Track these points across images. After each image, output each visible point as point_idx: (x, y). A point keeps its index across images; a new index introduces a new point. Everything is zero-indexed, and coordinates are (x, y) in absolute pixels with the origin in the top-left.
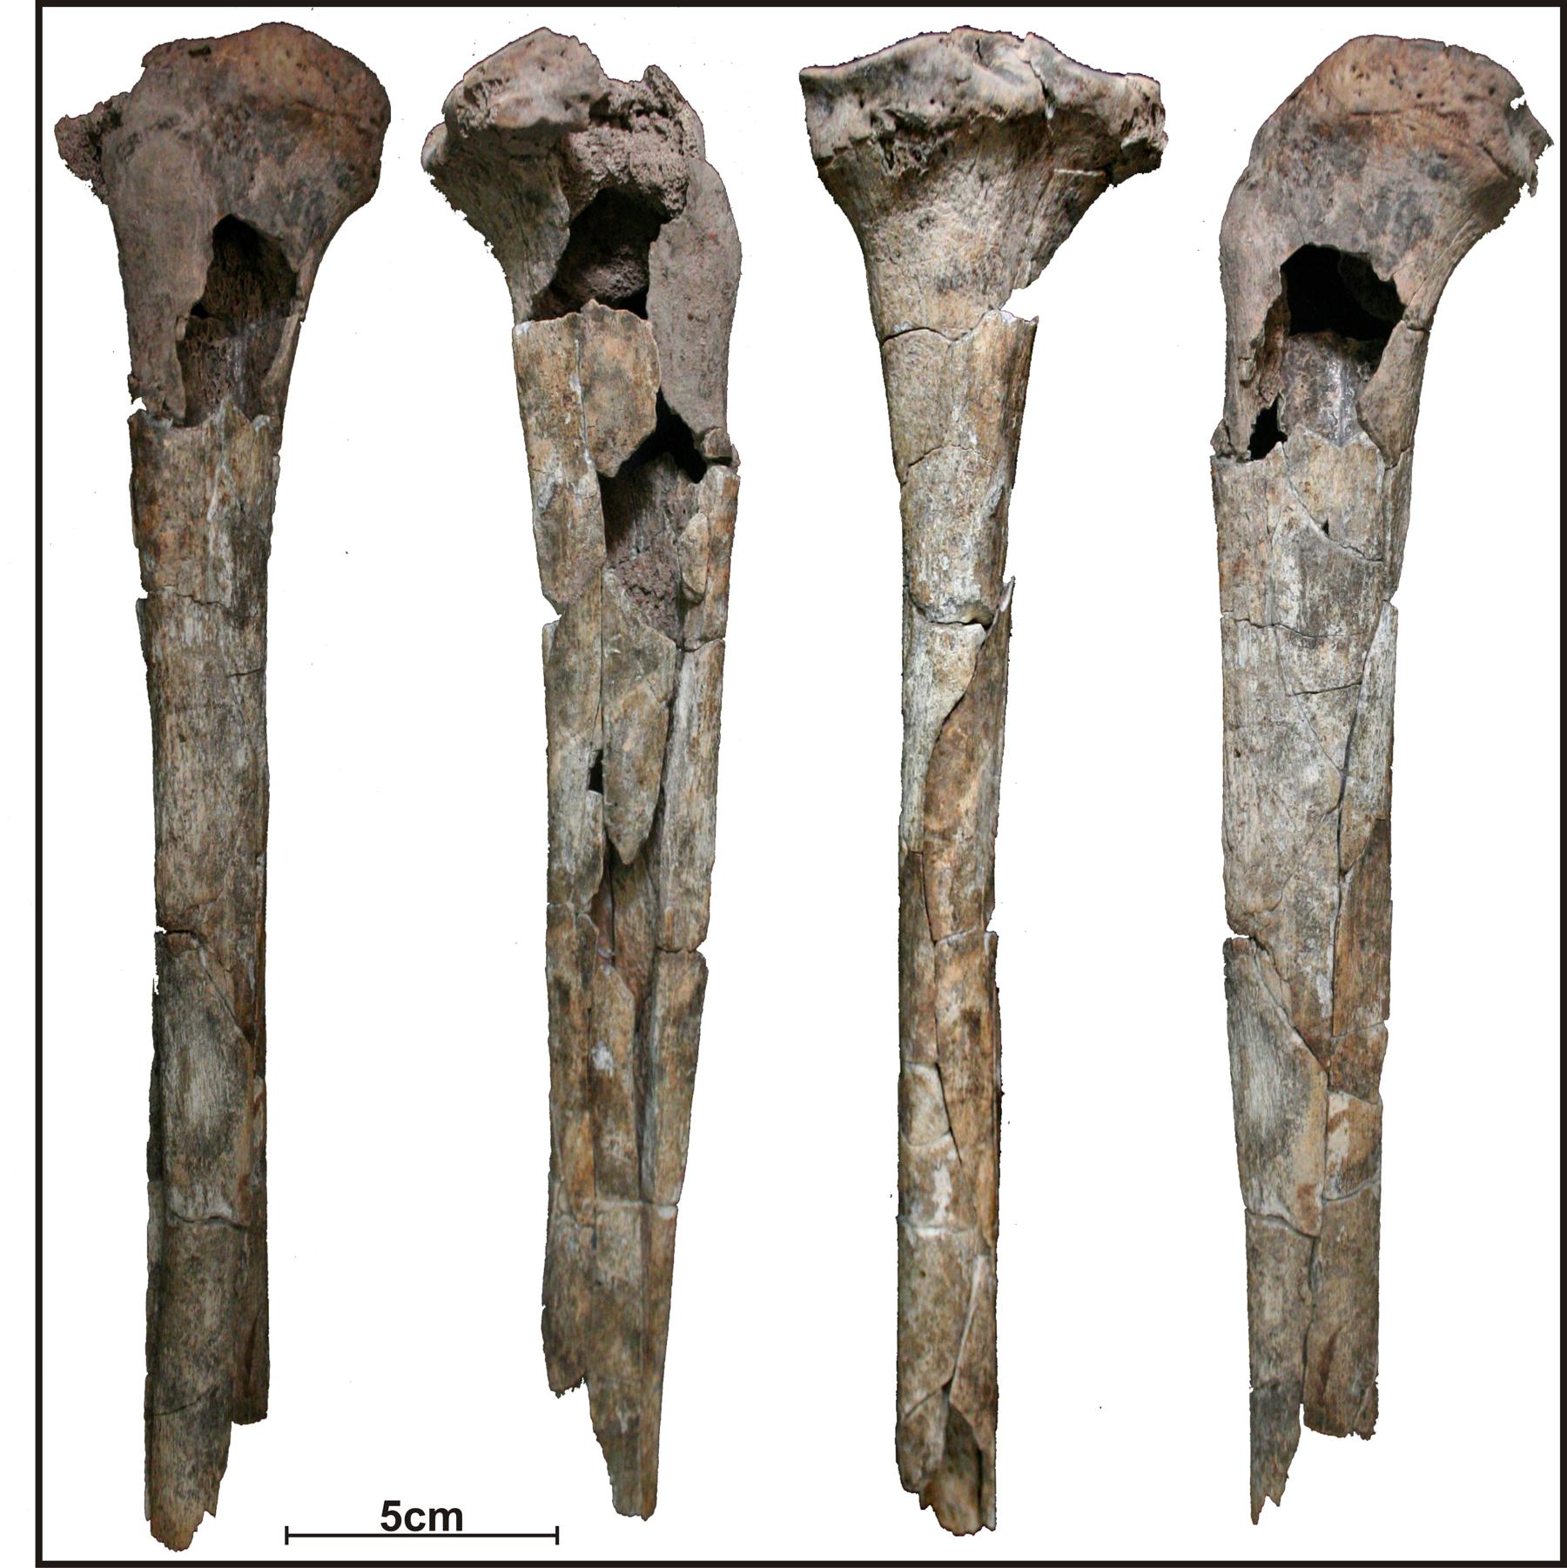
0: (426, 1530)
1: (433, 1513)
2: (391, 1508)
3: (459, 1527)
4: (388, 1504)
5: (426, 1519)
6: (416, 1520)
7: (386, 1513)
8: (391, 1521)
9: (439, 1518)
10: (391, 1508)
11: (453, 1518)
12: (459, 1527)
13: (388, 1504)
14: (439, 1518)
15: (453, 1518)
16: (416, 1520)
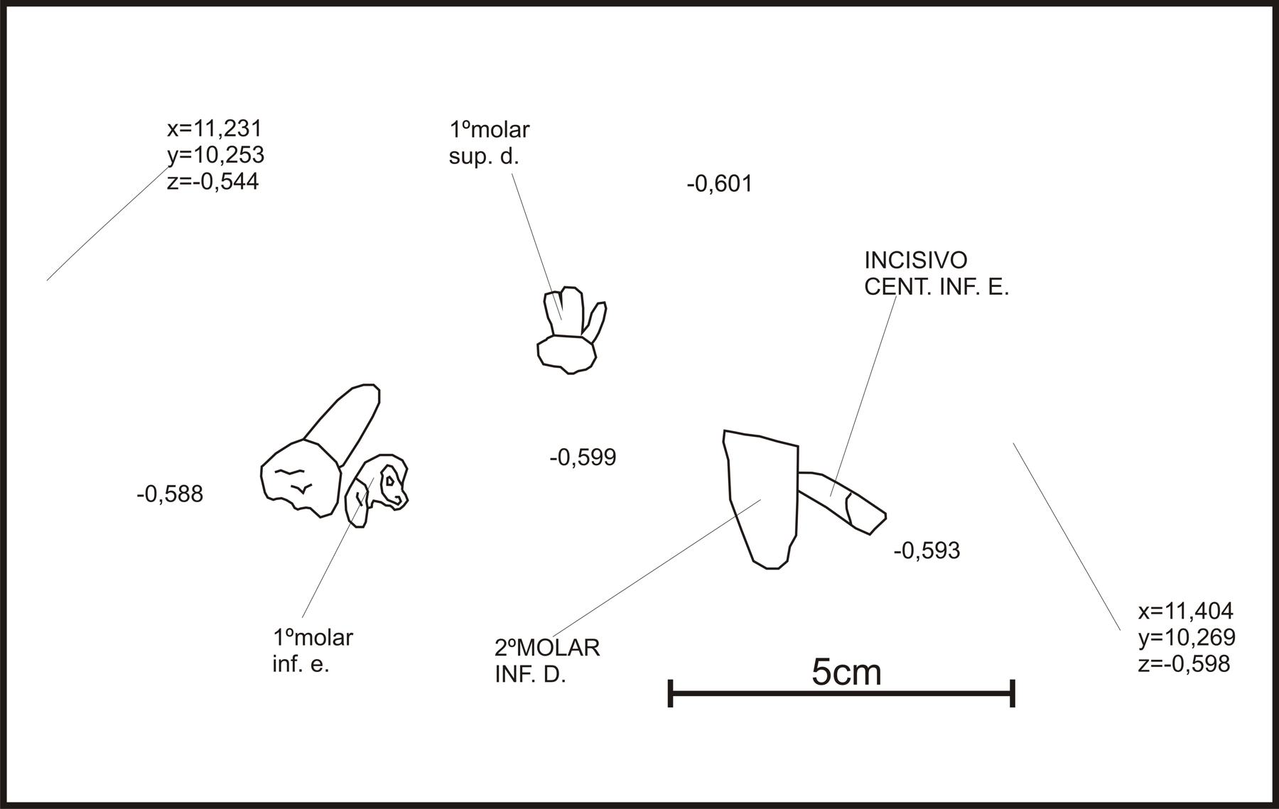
0: (850, 687)
1: (856, 668)
2: (821, 664)
3: (879, 683)
4: (818, 660)
5: (851, 674)
6: (843, 675)
7: (816, 669)
8: (822, 676)
9: (861, 672)
10: (821, 664)
11: (873, 672)
12: (879, 683)
13: (818, 660)
14: (861, 672)
15: (873, 672)
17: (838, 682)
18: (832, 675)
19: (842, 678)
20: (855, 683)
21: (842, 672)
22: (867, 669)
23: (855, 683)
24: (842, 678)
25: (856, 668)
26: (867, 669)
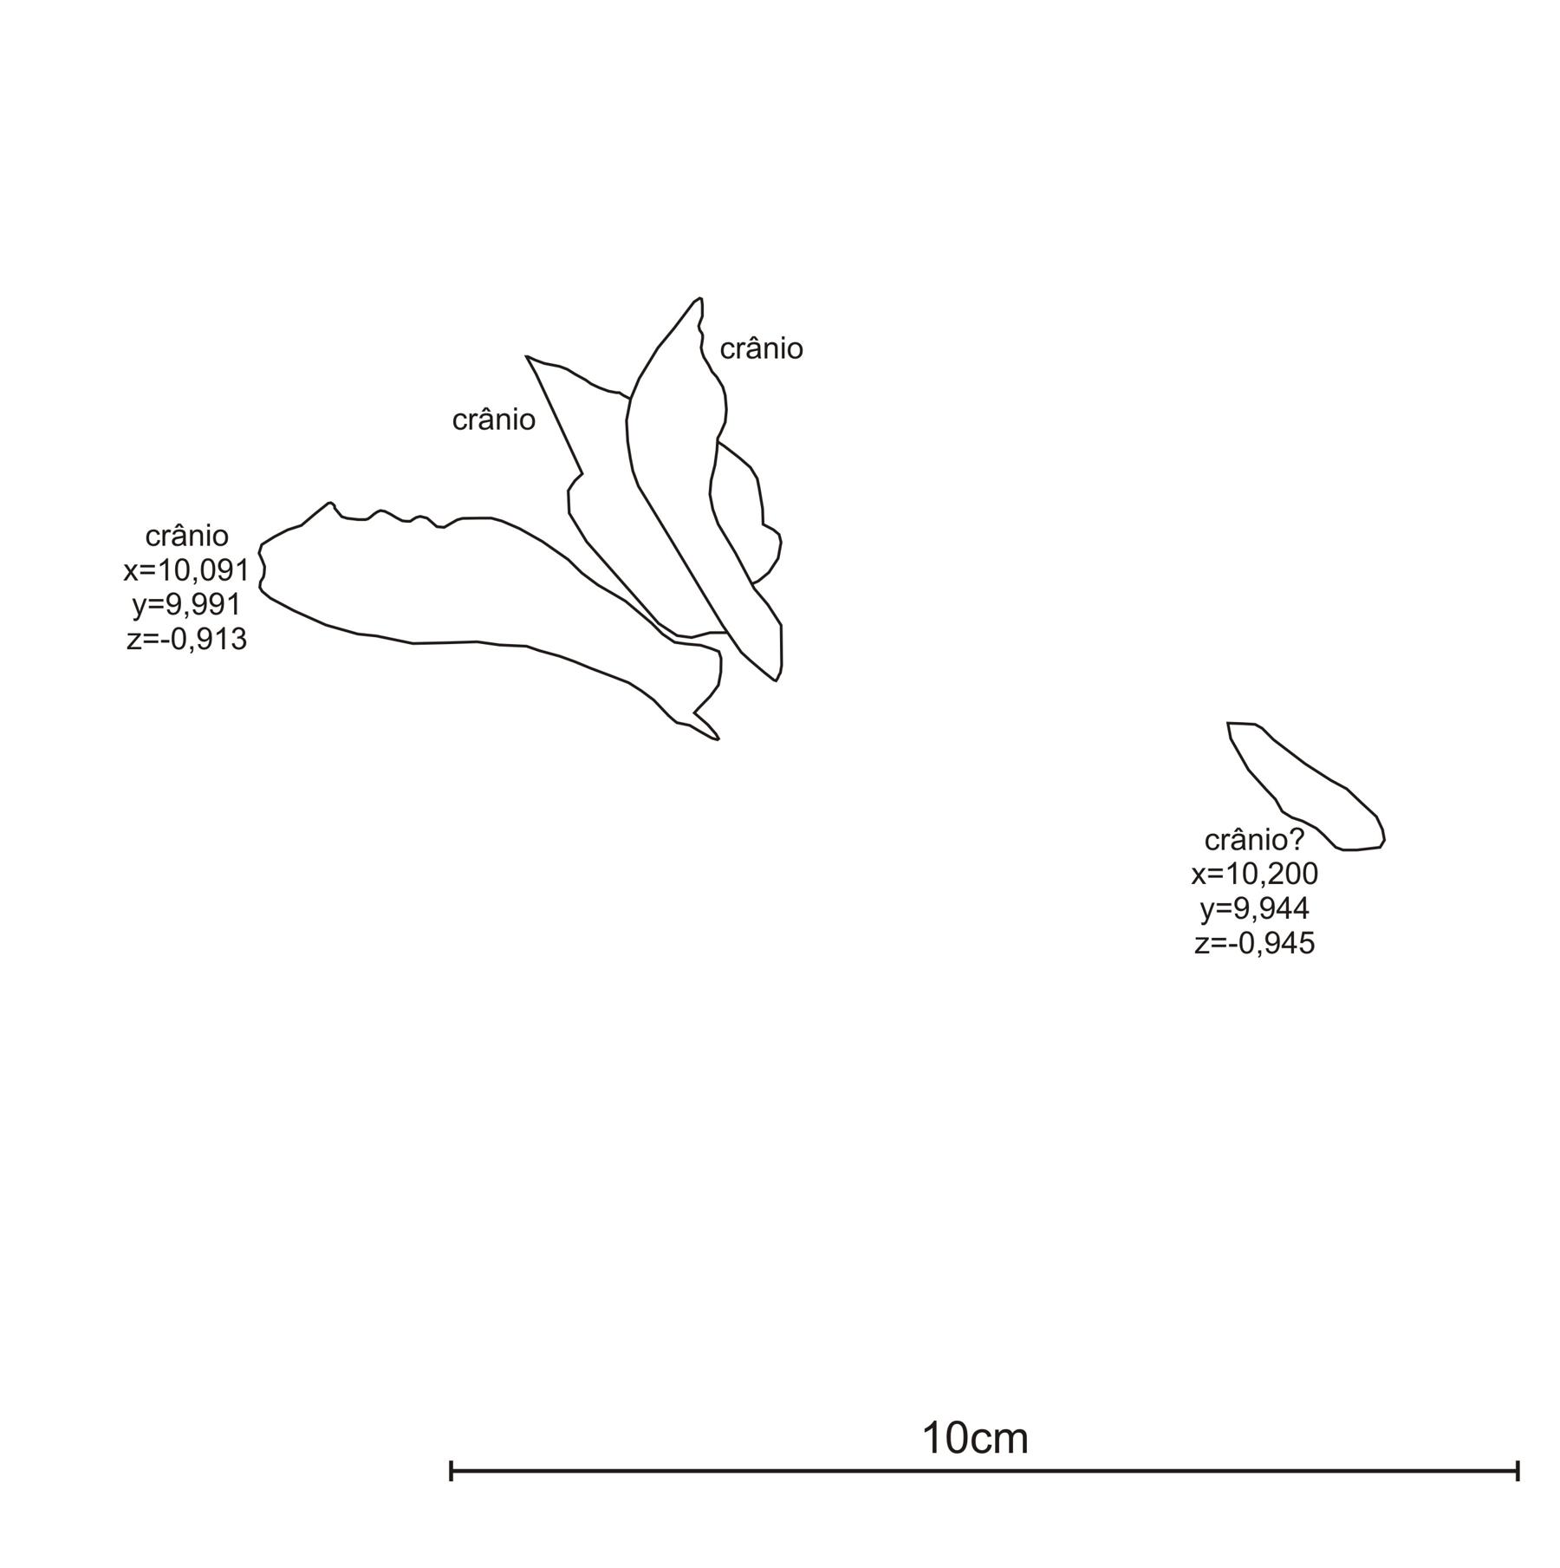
1: (998, 1434)
5: (992, 1440)
6: (982, 1441)
9: (1004, 1438)
11: (1018, 1438)
14: (1004, 1438)
15: (1018, 1438)
16: (982, 1441)
17: (973, 1446)
18: (970, 1440)
19: (981, 1447)
20: (997, 1451)
21: (981, 1436)
22: (1011, 1435)
23: (997, 1451)
24: (981, 1447)
25: (998, 1434)
26: (1011, 1435)
